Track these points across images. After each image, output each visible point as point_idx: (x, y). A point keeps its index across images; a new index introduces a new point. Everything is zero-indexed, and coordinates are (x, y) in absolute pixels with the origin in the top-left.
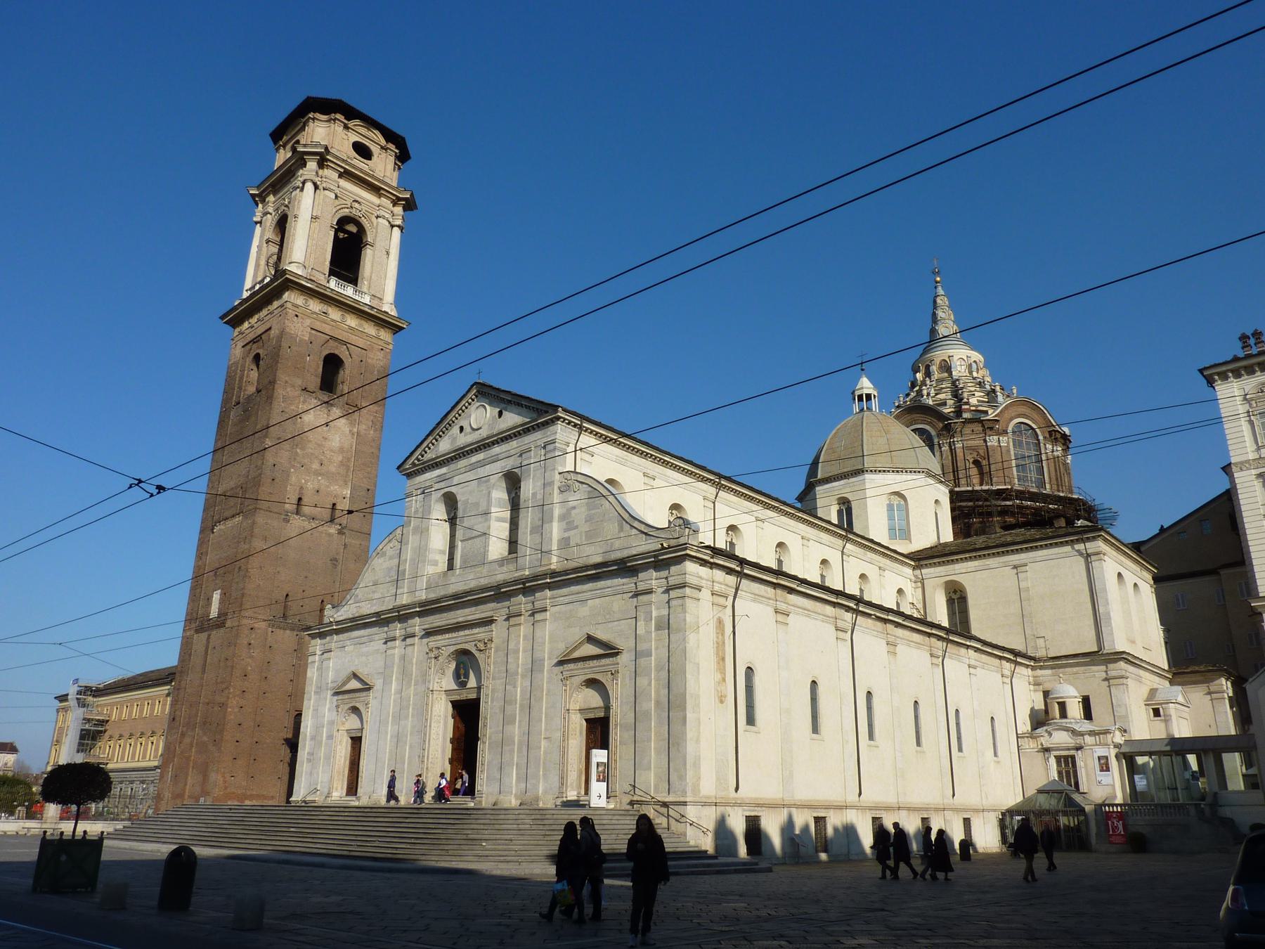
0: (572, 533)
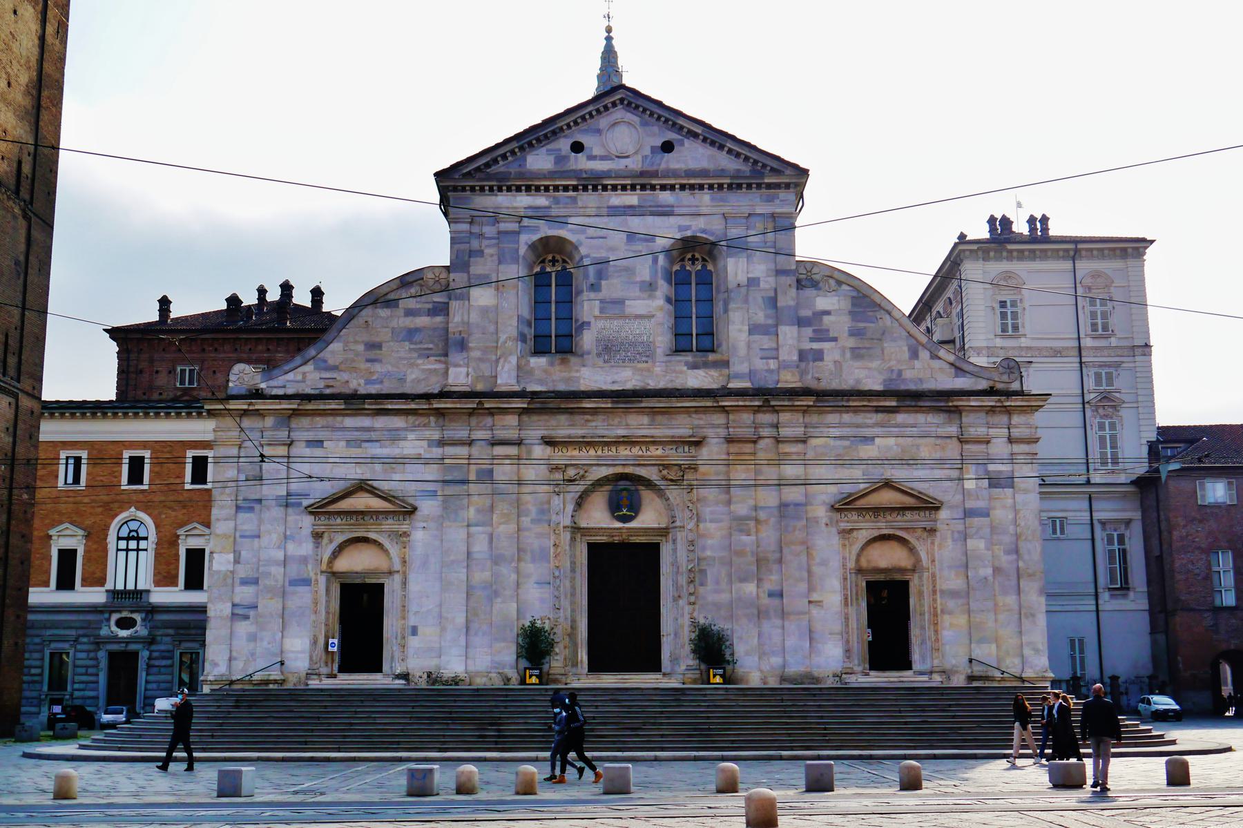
0: (826, 346)
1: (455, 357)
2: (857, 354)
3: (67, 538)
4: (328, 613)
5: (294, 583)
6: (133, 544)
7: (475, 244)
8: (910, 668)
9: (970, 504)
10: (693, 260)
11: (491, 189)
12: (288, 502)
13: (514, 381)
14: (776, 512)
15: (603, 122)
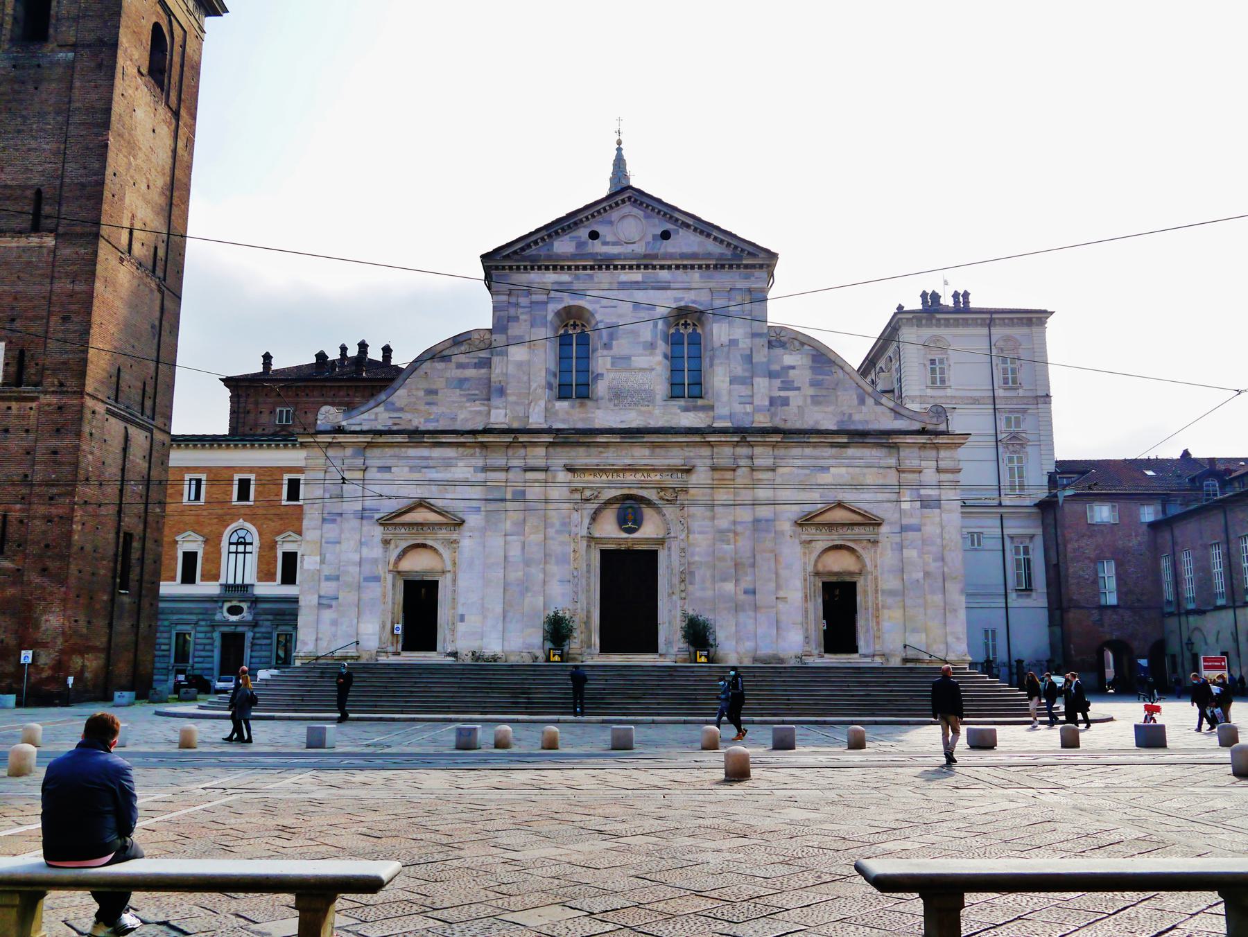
1: (496, 401)
2: (816, 400)
3: (191, 542)
4: (394, 603)
5: (366, 579)
6: (241, 548)
7: (512, 311)
8: (856, 652)
9: (905, 521)
10: (686, 325)
11: (525, 268)
12: (362, 515)
13: (542, 420)
14: (750, 525)
15: (615, 215)
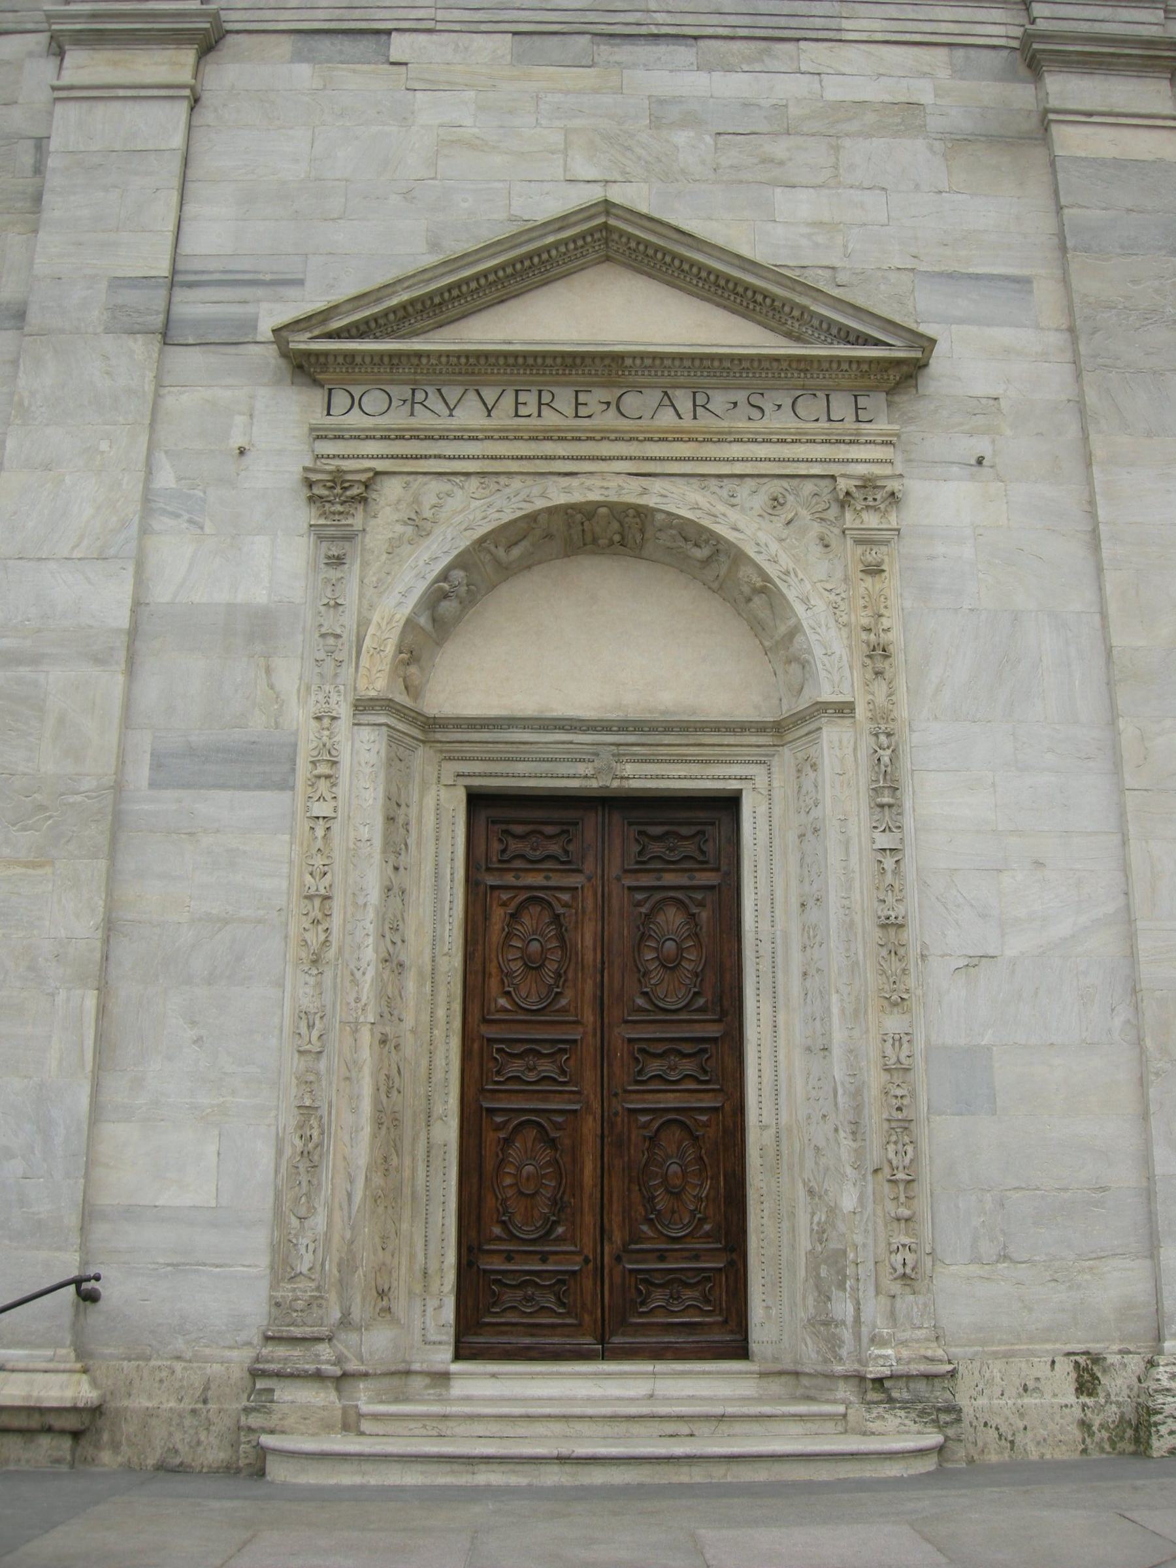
4: (393, 964)
5: (172, 769)
